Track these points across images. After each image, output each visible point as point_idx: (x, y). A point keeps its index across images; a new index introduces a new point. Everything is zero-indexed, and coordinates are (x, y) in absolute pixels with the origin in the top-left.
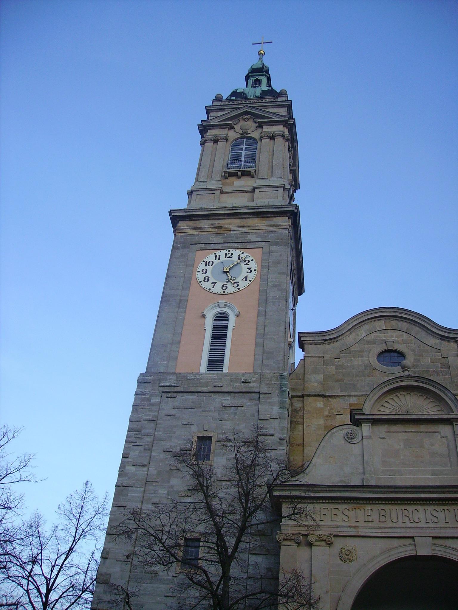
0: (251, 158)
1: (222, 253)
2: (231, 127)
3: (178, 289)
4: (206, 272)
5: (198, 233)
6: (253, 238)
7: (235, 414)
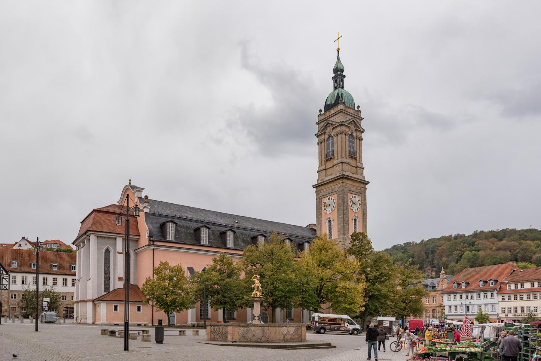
1: (327, 198)
2: (325, 133)
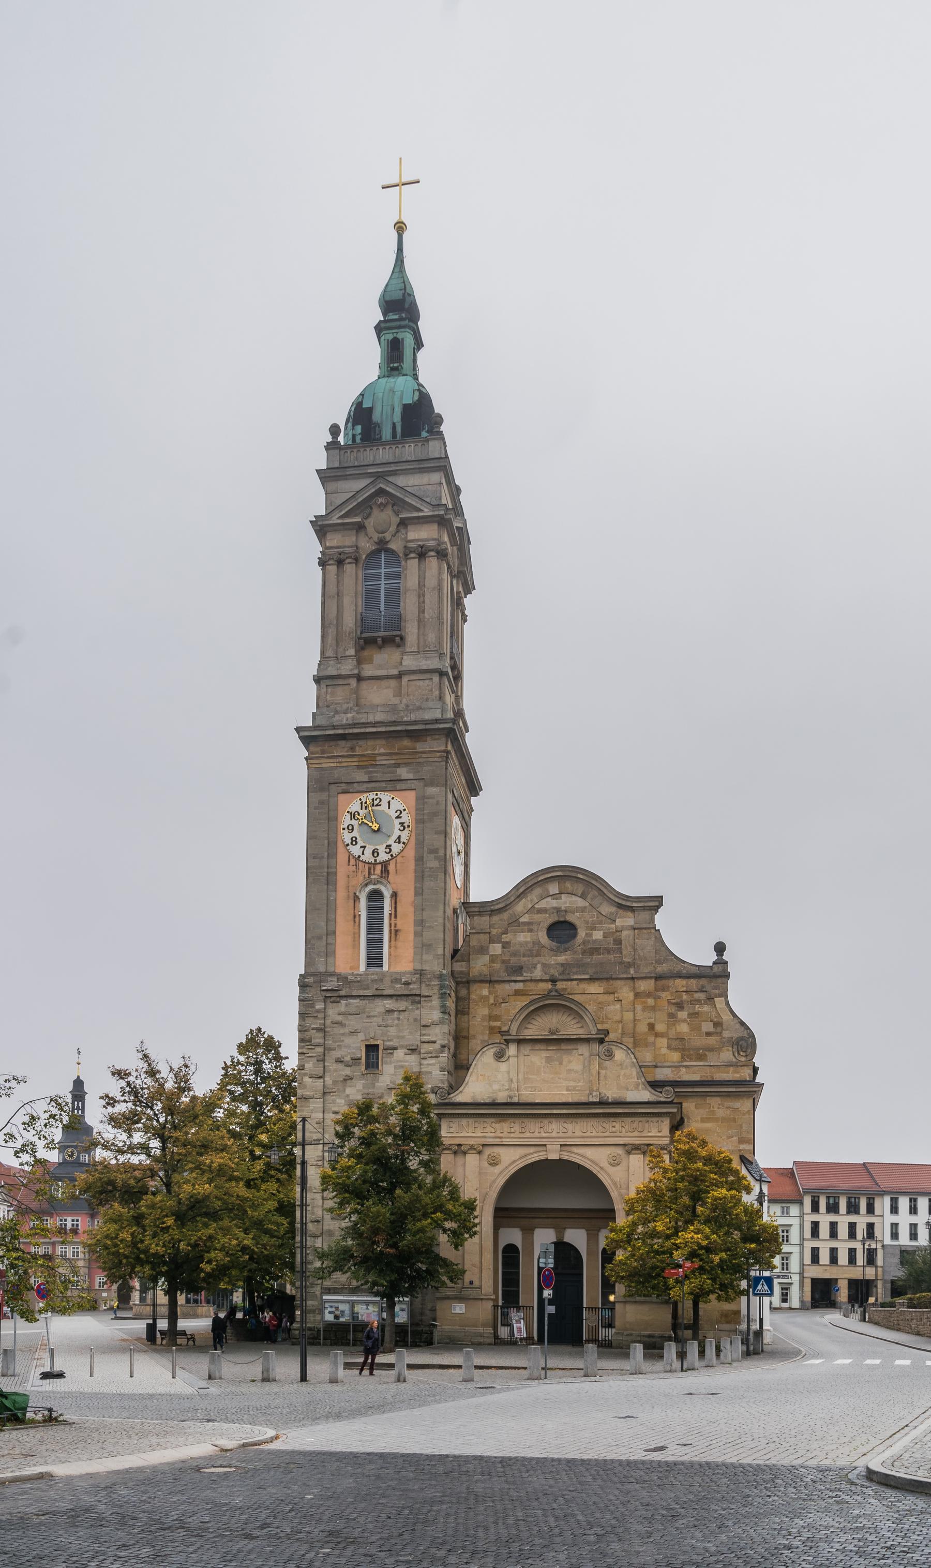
0: (394, 596)
2: (360, 528)
3: (323, 857)
4: (353, 830)
5: (336, 765)
6: (403, 773)
7: (399, 1019)
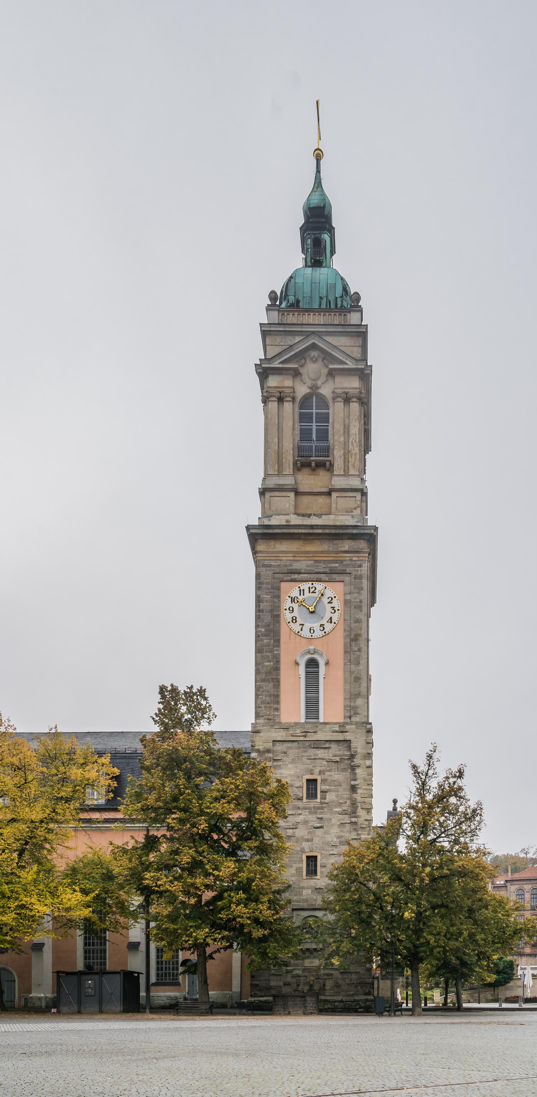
1: (305, 586)
2: (296, 374)
4: (293, 611)
